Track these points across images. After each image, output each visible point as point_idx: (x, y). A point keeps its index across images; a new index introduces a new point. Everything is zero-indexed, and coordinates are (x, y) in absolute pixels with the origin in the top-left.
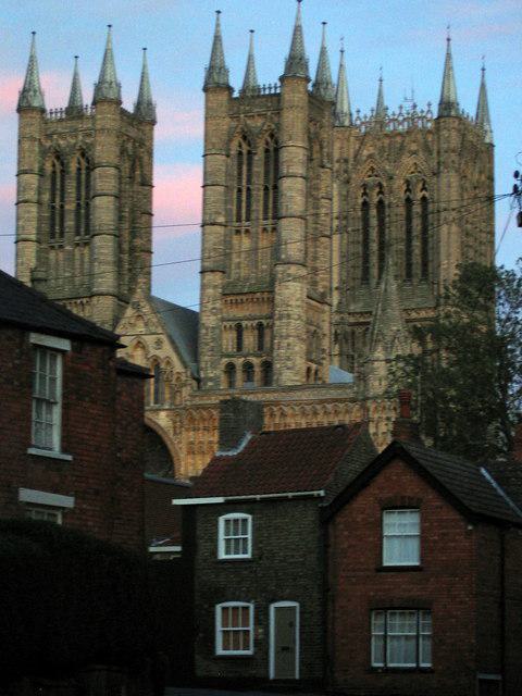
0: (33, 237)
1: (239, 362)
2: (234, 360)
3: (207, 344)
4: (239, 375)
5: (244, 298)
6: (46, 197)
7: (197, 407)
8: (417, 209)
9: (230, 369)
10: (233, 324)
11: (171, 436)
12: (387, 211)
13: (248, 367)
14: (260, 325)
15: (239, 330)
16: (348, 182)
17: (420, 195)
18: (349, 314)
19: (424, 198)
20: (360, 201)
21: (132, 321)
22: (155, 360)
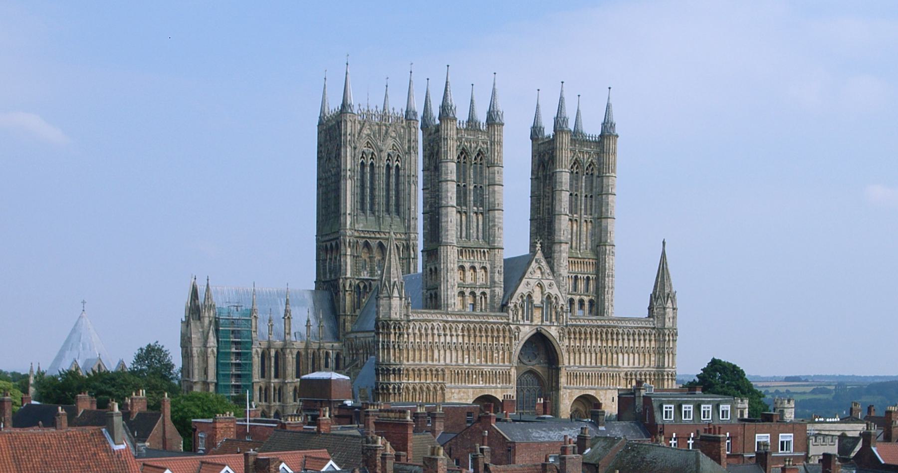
0: (455, 205)
1: (577, 298)
2: (573, 297)
3: (563, 286)
4: (577, 306)
5: (579, 261)
7: (572, 326)
8: (393, 171)
9: (571, 302)
10: (574, 275)
11: (558, 341)
12: (376, 170)
13: (581, 302)
14: (588, 278)
16: (355, 148)
17: (395, 164)
18: (355, 230)
19: (397, 166)
20: (360, 161)
22: (548, 296)
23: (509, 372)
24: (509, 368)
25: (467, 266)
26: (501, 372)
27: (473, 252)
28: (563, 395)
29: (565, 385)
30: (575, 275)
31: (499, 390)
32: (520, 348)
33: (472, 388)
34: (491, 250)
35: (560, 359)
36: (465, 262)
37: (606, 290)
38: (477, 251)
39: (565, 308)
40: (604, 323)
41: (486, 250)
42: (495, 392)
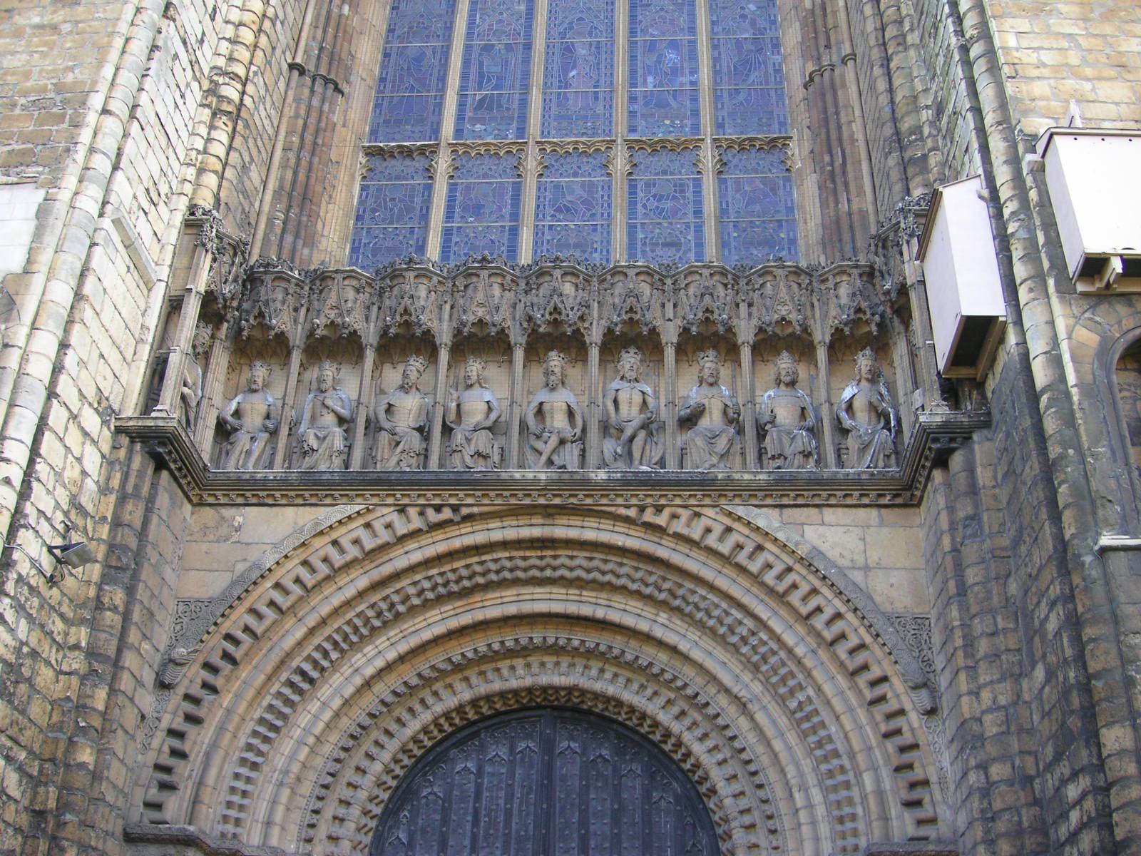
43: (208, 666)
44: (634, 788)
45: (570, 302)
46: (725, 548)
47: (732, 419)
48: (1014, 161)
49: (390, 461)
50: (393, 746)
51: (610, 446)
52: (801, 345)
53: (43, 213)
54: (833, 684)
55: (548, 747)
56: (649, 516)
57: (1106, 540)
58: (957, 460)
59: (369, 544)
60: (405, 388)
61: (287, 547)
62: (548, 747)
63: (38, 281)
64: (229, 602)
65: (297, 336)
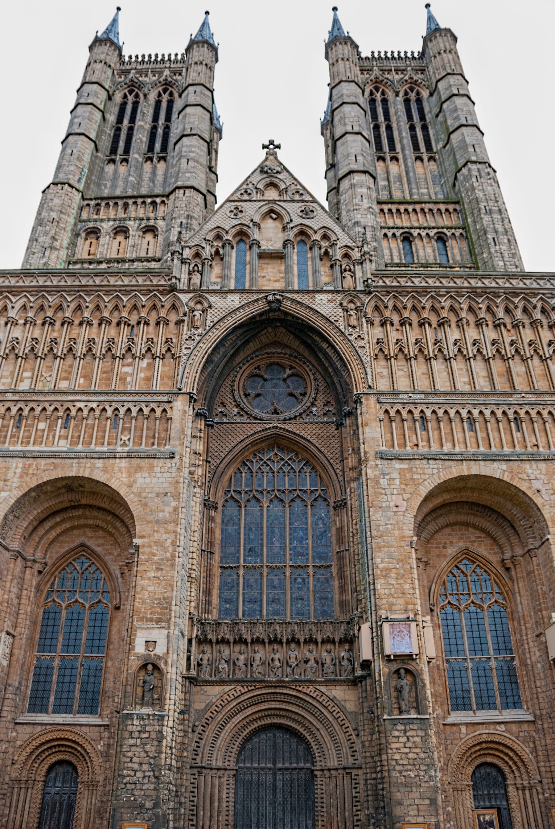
5: (410, 208)
6: (112, 118)
7: (388, 290)
11: (343, 330)
15: (407, 238)
21: (261, 186)
22: (302, 233)
23: (164, 410)
24: (165, 398)
25: (106, 227)
26: (134, 411)
27: (126, 206)
28: (378, 483)
29: (383, 448)
30: (401, 231)
31: (124, 463)
32: (206, 346)
33: (24, 455)
34: (172, 197)
35: (357, 372)
36: (102, 220)
37: (489, 236)
38: (135, 203)
39: (356, 254)
40: (494, 285)
41: (158, 200)
42: (105, 470)
43: (203, 726)
44: (294, 746)
45: (279, 632)
46: (314, 696)
47: (316, 662)
48: (376, 622)
49: (239, 675)
50: (241, 738)
51: (289, 669)
52: (333, 642)
53: (168, 636)
54: (337, 728)
55: (275, 736)
56: (298, 688)
57: (385, 717)
58: (363, 683)
59: (236, 695)
60: (241, 653)
61: (218, 697)
62: (275, 736)
63: (170, 655)
64: (205, 710)
65: (214, 640)
